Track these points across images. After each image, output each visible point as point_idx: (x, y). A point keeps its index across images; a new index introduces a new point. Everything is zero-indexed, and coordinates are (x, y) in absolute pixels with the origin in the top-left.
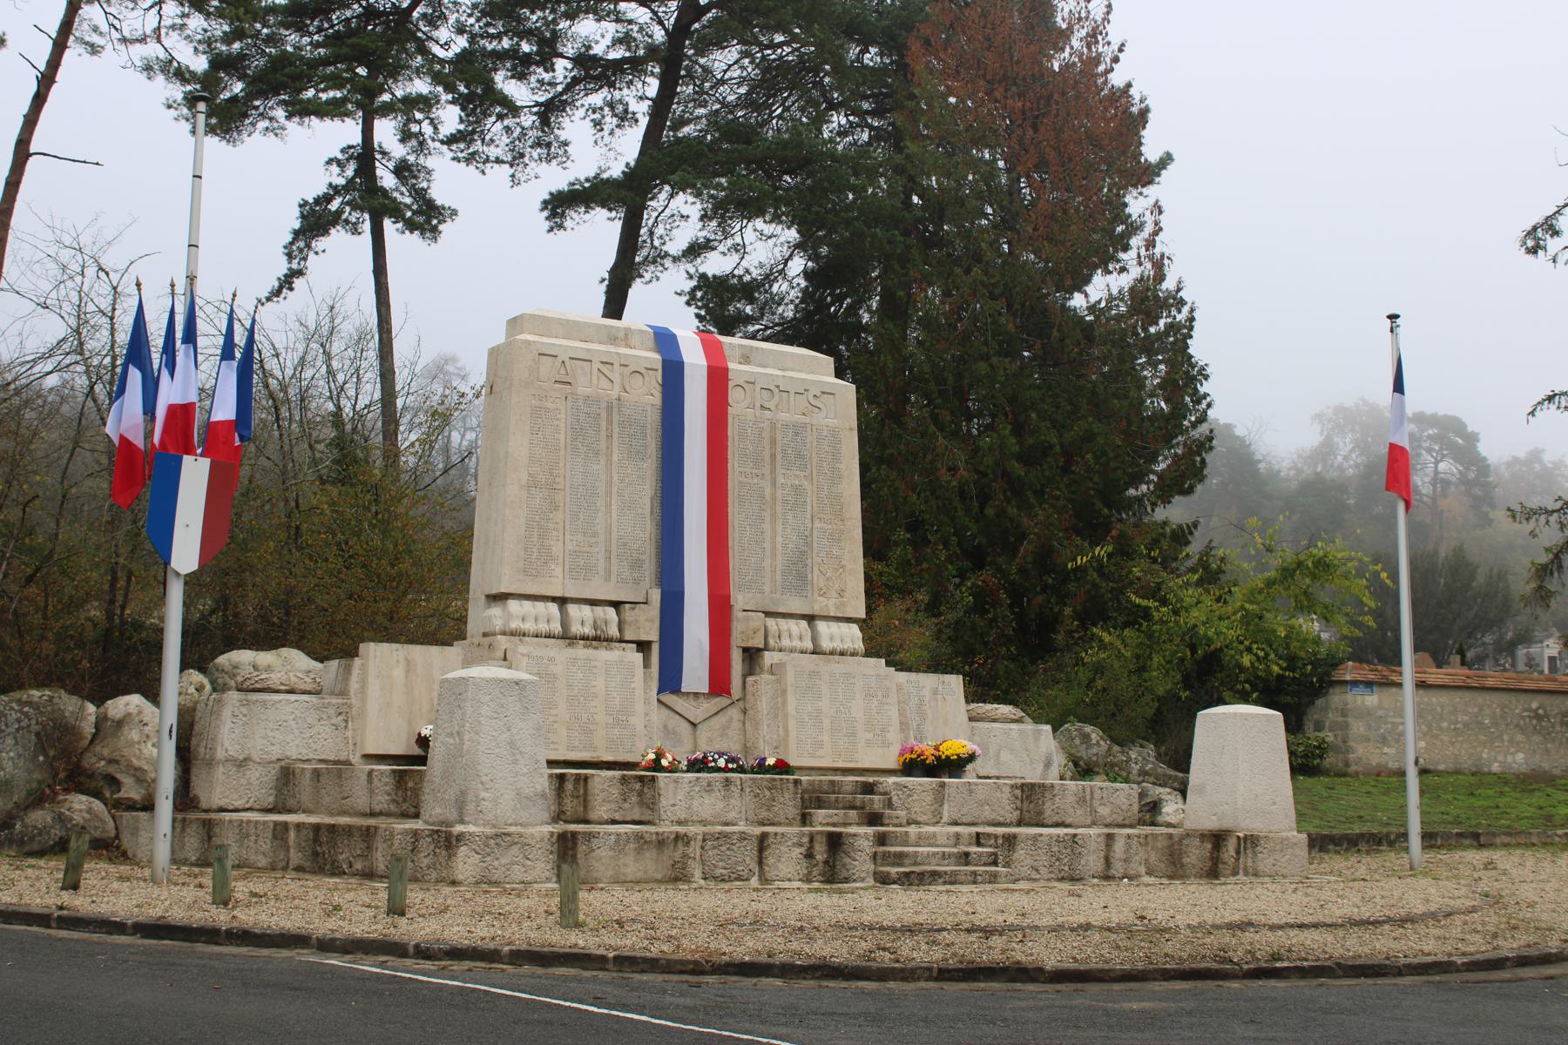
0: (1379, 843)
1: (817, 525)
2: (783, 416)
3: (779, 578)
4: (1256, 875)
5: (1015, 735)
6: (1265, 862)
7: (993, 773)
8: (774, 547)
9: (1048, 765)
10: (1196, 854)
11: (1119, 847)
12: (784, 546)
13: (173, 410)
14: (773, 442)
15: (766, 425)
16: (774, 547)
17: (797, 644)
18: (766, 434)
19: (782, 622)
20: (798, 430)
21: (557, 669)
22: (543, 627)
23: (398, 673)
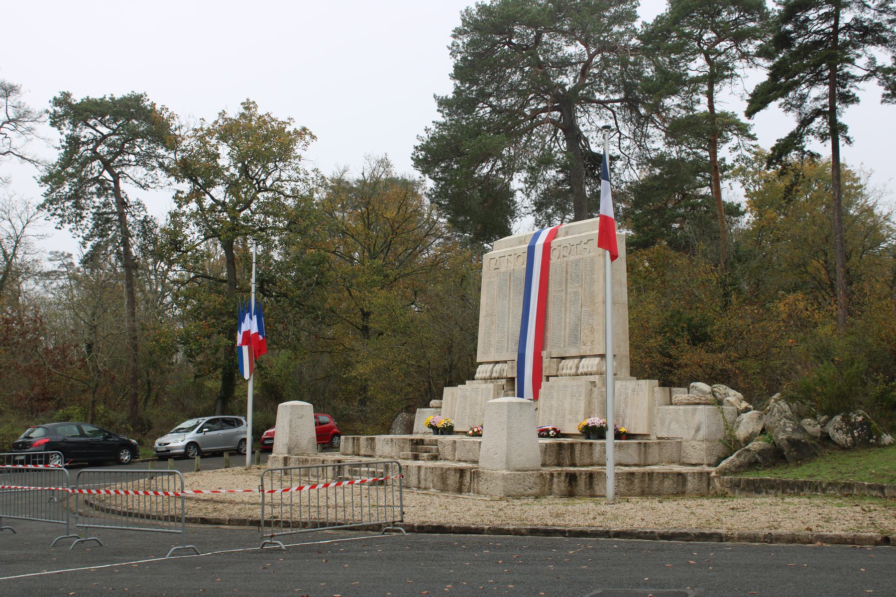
0: (816, 490)
1: (584, 309)
2: (572, 258)
3: (567, 339)
4: (478, 493)
5: (681, 412)
6: (483, 487)
7: (665, 435)
8: (565, 325)
9: (698, 430)
10: (453, 479)
11: (423, 472)
12: (570, 323)
13: (244, 333)
14: (567, 273)
15: (564, 265)
16: (565, 325)
17: (568, 371)
18: (564, 270)
19: (567, 361)
20: (577, 263)
21: (468, 393)
22: (484, 375)
23: (450, 398)
